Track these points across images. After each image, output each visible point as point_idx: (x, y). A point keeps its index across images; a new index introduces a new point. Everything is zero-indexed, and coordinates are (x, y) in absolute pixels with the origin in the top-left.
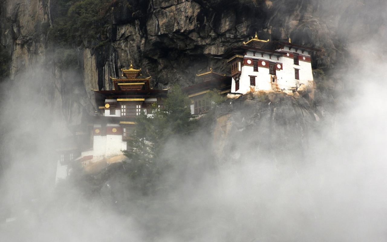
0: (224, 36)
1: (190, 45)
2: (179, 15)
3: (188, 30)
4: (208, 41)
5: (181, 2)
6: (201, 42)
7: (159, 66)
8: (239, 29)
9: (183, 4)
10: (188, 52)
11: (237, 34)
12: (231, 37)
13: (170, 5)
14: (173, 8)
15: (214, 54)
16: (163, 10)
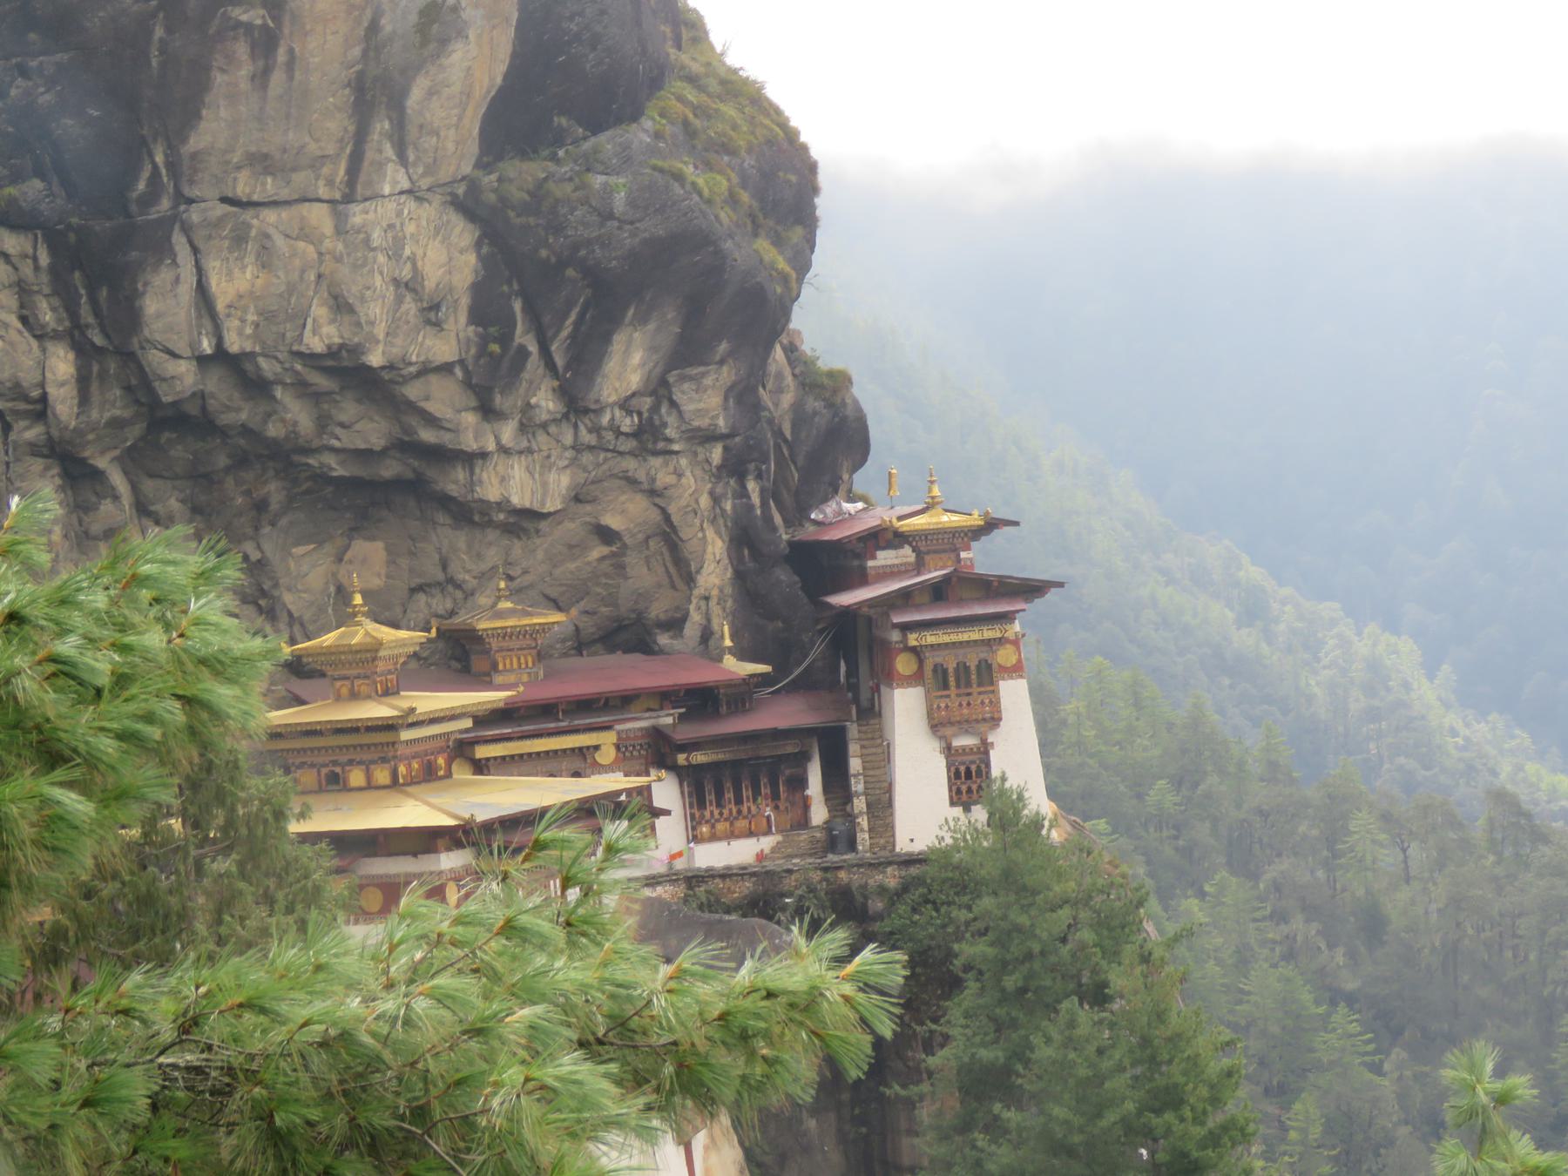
0: (592, 416)
1: (357, 427)
2: (355, 267)
3: (414, 359)
4: (508, 432)
5: (368, 193)
6: (470, 431)
7: (107, 506)
8: (683, 392)
9: (385, 210)
10: (330, 460)
11: (661, 417)
12: (625, 429)
13: (296, 197)
14: (318, 215)
15: (527, 505)
16: (247, 216)
